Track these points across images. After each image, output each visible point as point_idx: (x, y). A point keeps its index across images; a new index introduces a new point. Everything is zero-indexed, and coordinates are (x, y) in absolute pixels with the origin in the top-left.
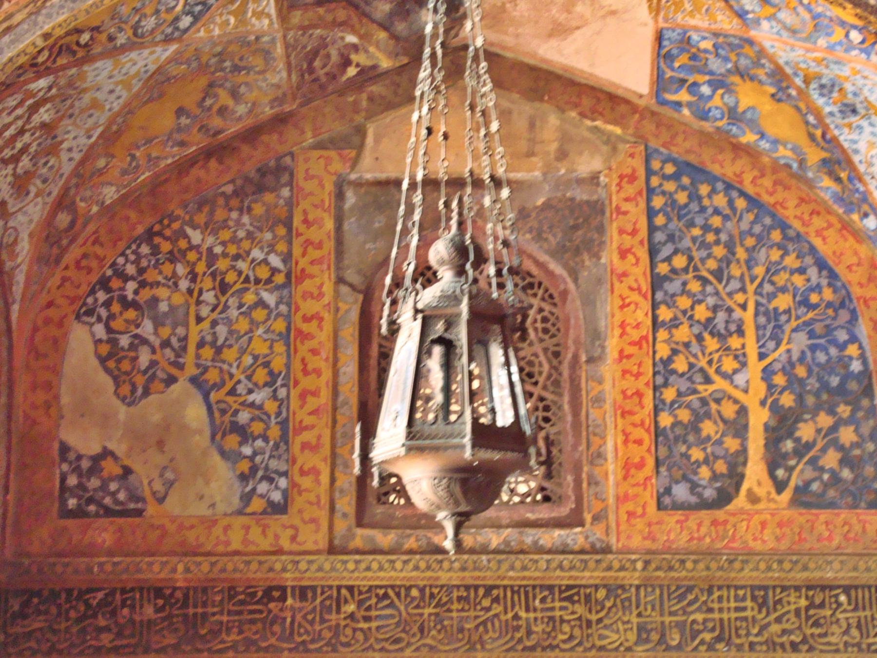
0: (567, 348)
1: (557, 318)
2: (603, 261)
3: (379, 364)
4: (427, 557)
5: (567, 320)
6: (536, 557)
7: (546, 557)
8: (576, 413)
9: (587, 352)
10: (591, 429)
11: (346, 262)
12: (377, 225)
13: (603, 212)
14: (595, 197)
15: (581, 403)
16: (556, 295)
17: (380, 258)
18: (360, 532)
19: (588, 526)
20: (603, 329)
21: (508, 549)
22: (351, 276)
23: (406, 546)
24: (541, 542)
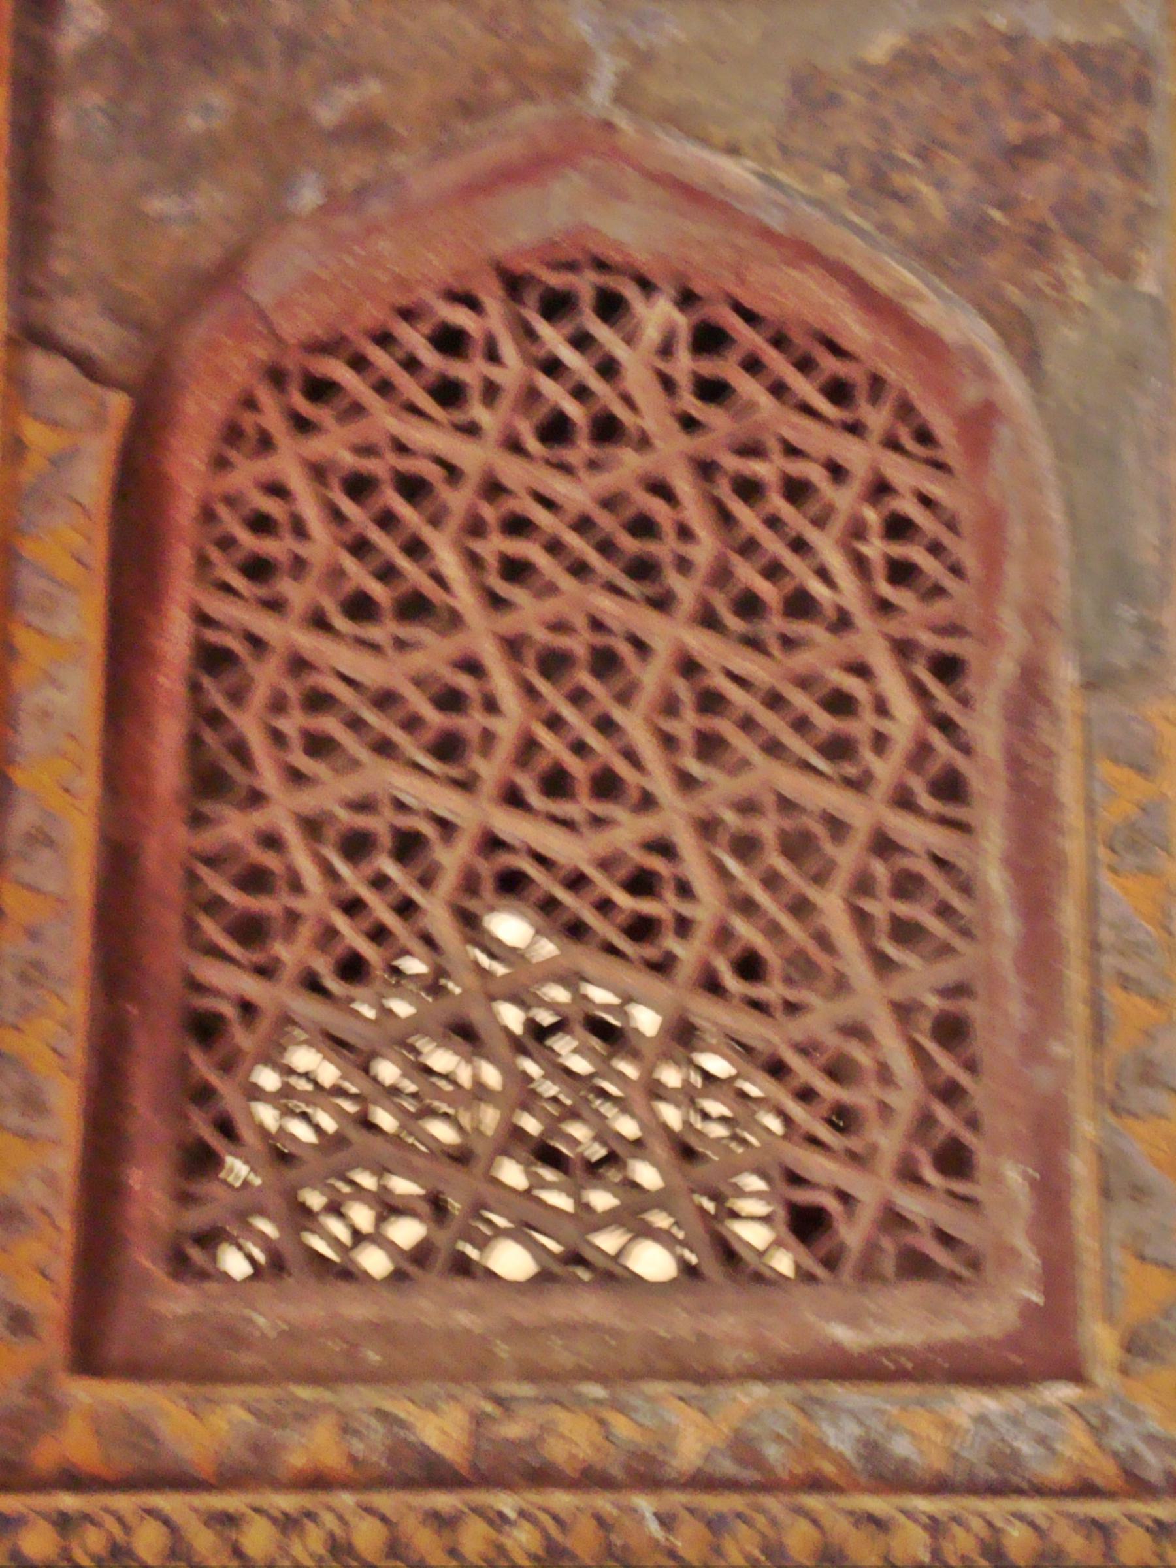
0: (991, 635)
1: (952, 526)
2: (1148, 285)
3: (195, 688)
4: (384, 1501)
5: (992, 527)
6: (877, 1504)
7: (924, 1505)
8: (1036, 903)
9: (1081, 646)
10: (1109, 961)
11: (61, 267)
12: (195, 123)
13: (1142, 91)
14: (1112, 31)
15: (1061, 863)
16: (942, 425)
17: (207, 254)
18: (84, 1392)
19: (1104, 1377)
20: (1150, 557)
21: (749, 1475)
22: (85, 323)
23: (297, 1461)
24: (901, 1447)
